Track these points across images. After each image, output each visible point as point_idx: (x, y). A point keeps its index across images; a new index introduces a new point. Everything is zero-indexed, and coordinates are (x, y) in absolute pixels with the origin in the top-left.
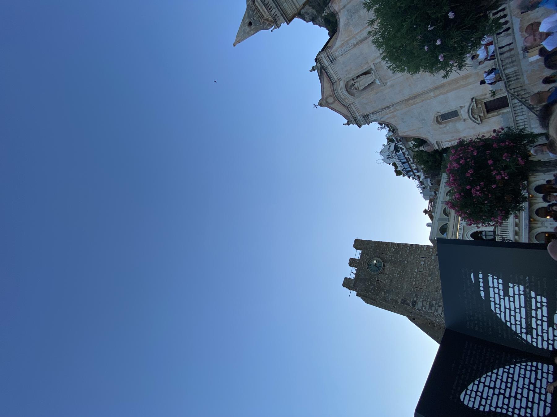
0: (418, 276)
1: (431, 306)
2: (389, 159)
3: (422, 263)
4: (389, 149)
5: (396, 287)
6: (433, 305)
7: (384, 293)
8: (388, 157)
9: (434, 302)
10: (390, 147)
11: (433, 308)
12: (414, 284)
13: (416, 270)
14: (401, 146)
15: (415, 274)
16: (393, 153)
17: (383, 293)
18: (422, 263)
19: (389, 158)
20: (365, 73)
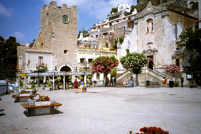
0: (64, 38)
1: (54, 43)
2: (121, 8)
3: (70, 39)
4: (127, 8)
5: (58, 30)
6: (55, 44)
7: (54, 24)
8: (122, 7)
9: (56, 44)
10: (129, 9)
11: (54, 44)
12: (61, 36)
13: (66, 37)
14: (126, 19)
15: (65, 37)
16: (124, 11)
17: (54, 23)
18: (70, 39)
19: (121, 9)
20: (153, 28)
